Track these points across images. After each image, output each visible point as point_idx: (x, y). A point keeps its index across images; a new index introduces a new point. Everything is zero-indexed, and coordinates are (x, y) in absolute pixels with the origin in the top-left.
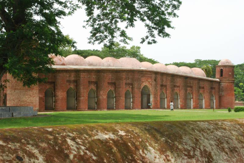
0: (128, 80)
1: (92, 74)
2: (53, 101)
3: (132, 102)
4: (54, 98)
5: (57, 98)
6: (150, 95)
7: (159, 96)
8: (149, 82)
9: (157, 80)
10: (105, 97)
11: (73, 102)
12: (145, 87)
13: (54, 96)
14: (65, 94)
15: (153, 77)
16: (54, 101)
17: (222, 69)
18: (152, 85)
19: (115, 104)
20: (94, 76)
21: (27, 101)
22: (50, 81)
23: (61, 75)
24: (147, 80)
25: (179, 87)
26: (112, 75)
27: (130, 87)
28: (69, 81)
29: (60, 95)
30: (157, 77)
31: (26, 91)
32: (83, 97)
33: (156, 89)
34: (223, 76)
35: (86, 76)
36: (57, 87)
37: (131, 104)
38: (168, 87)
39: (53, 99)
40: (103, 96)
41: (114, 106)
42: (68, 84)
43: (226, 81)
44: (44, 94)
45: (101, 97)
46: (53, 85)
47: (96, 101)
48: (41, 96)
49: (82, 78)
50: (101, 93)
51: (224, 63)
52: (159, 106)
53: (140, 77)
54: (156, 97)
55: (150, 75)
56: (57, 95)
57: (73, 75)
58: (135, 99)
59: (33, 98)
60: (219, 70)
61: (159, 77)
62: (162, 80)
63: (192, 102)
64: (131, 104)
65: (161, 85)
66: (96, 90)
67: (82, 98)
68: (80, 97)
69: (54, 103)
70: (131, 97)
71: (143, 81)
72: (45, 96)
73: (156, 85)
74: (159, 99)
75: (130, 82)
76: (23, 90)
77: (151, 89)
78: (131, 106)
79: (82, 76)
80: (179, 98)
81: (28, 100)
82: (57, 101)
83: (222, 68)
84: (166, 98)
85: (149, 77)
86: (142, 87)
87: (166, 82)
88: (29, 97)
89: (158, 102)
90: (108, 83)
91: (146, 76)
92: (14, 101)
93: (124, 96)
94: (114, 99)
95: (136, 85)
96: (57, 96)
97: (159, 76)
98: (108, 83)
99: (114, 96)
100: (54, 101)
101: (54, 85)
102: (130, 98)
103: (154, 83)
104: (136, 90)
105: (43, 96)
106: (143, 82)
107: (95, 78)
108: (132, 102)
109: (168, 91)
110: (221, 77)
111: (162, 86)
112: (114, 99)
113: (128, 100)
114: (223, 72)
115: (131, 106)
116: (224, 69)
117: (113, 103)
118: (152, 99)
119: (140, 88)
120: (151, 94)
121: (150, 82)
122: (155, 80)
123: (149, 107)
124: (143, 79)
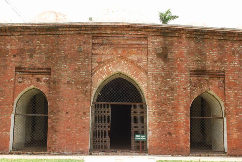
7: (181, 108)
9: (170, 56)
15: (150, 45)
24: (122, 57)
30: (172, 44)
33: (165, 83)
52: (182, 144)
53: (85, 47)
54: (171, 111)
55: (138, 38)
65: (196, 71)
71: (105, 58)
85: (130, 45)
87: (220, 60)
89: (182, 131)
91: (118, 44)
97: (185, 41)
106: (101, 63)
109: (231, 93)
121: (140, 60)
122: (163, 55)
124: (104, 53)
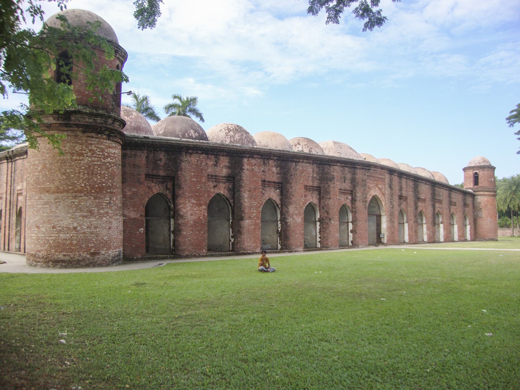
0: (345, 182)
1: (271, 162)
2: (170, 228)
3: (352, 232)
4: (172, 221)
5: (180, 221)
6: (379, 217)
8: (380, 189)
10: (299, 220)
11: (224, 232)
12: (375, 199)
13: (174, 217)
14: (202, 212)
16: (172, 229)
17: (476, 173)
18: (384, 195)
19: (318, 235)
20: (274, 169)
21: (79, 228)
22: (162, 173)
23: (194, 159)
25: (424, 200)
26: (313, 169)
27: (347, 198)
28: (214, 178)
29: (189, 213)
31: (75, 197)
32: (250, 218)
34: (480, 185)
35: (256, 169)
36: (180, 192)
37: (351, 235)
38: (409, 201)
39: (170, 224)
40: (296, 218)
41: (318, 240)
42: (211, 184)
43: (485, 193)
44: (142, 208)
45: (290, 220)
46: (170, 185)
47: (280, 229)
48: (133, 215)
49: (245, 171)
50: (291, 209)
51: (480, 163)
56: (181, 213)
57: (224, 161)
58: (359, 223)
59: (101, 218)
60: (472, 175)
61: (395, 178)
62: (401, 189)
63: (425, 229)
64: (351, 235)
66: (278, 202)
67: (247, 221)
68: (242, 219)
69: (172, 235)
70: (350, 220)
72: (146, 215)
73: (392, 195)
74: (396, 224)
75: (348, 188)
76: (65, 194)
77: (384, 204)
78: (351, 239)
79: (246, 167)
80: (424, 222)
81: (81, 226)
82: (180, 231)
83: (477, 171)
84: (407, 222)
86: (369, 198)
88: (86, 217)
90: (306, 188)
92: (38, 227)
93: (337, 217)
94: (318, 224)
95: (359, 195)
96: (182, 217)
98: (306, 188)
99: (318, 216)
100: (172, 229)
101: (174, 185)
102: (348, 222)
103: (387, 191)
104: (359, 204)
105: (141, 216)
107: (277, 173)
108: (352, 232)
110: (476, 187)
111: (401, 197)
112: (318, 223)
113: (344, 227)
114: (479, 177)
115: (351, 239)
116: (481, 173)
117: (315, 234)
118: (384, 225)
119: (366, 201)
120: (382, 214)
123: (379, 241)
